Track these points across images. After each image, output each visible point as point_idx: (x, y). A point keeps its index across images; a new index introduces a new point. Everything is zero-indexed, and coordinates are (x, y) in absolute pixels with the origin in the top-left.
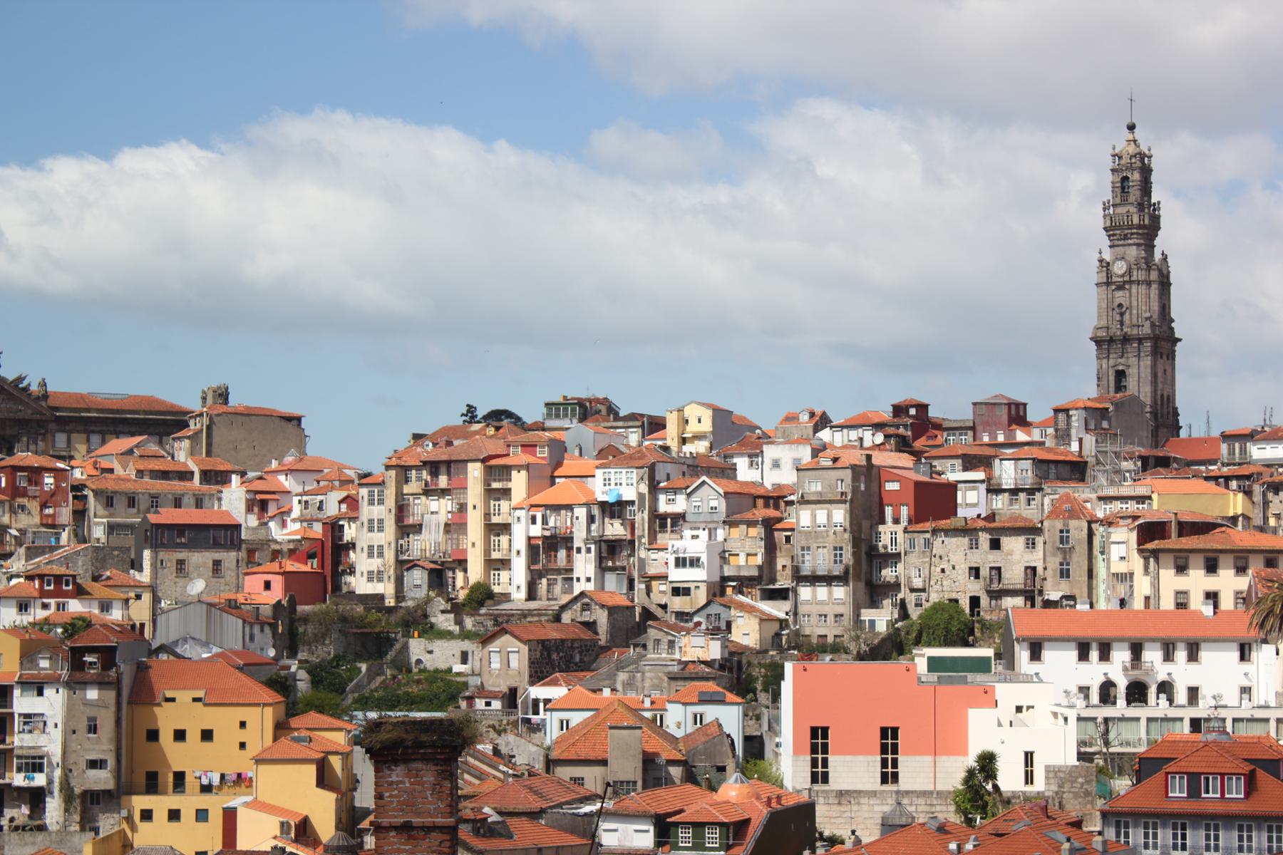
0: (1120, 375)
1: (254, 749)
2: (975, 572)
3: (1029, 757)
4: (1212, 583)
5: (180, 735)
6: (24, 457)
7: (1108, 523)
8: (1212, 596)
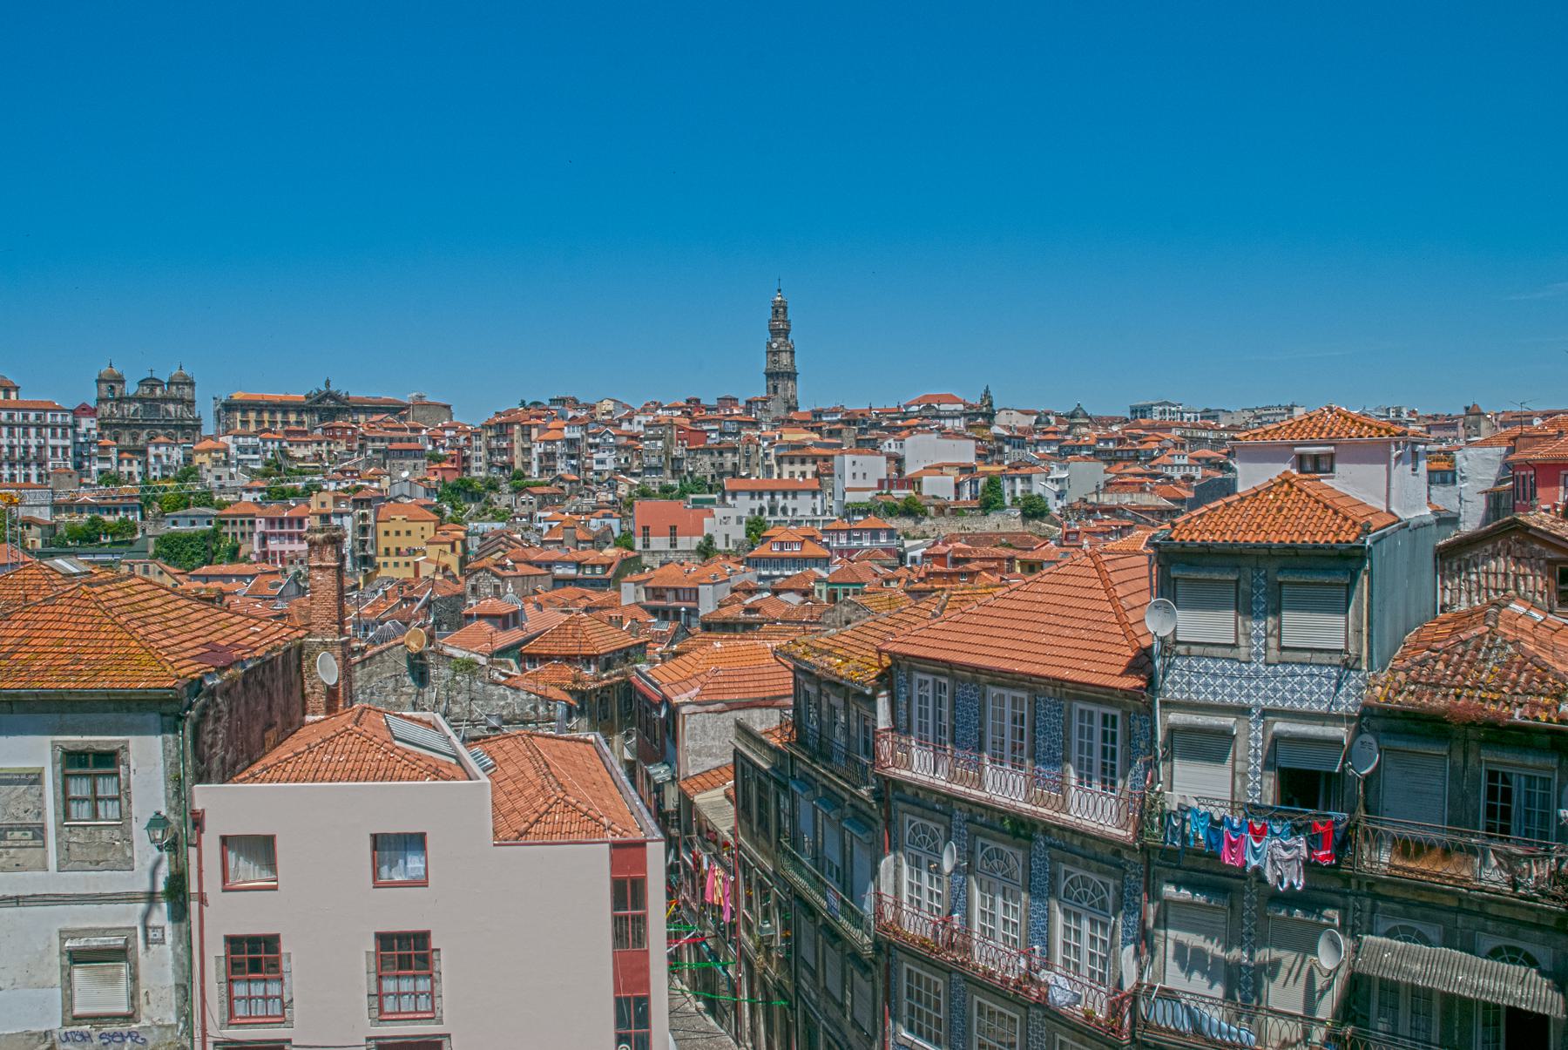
0: (775, 388)
1: (427, 538)
3: (727, 536)
5: (398, 533)
6: (340, 423)
8: (803, 474)
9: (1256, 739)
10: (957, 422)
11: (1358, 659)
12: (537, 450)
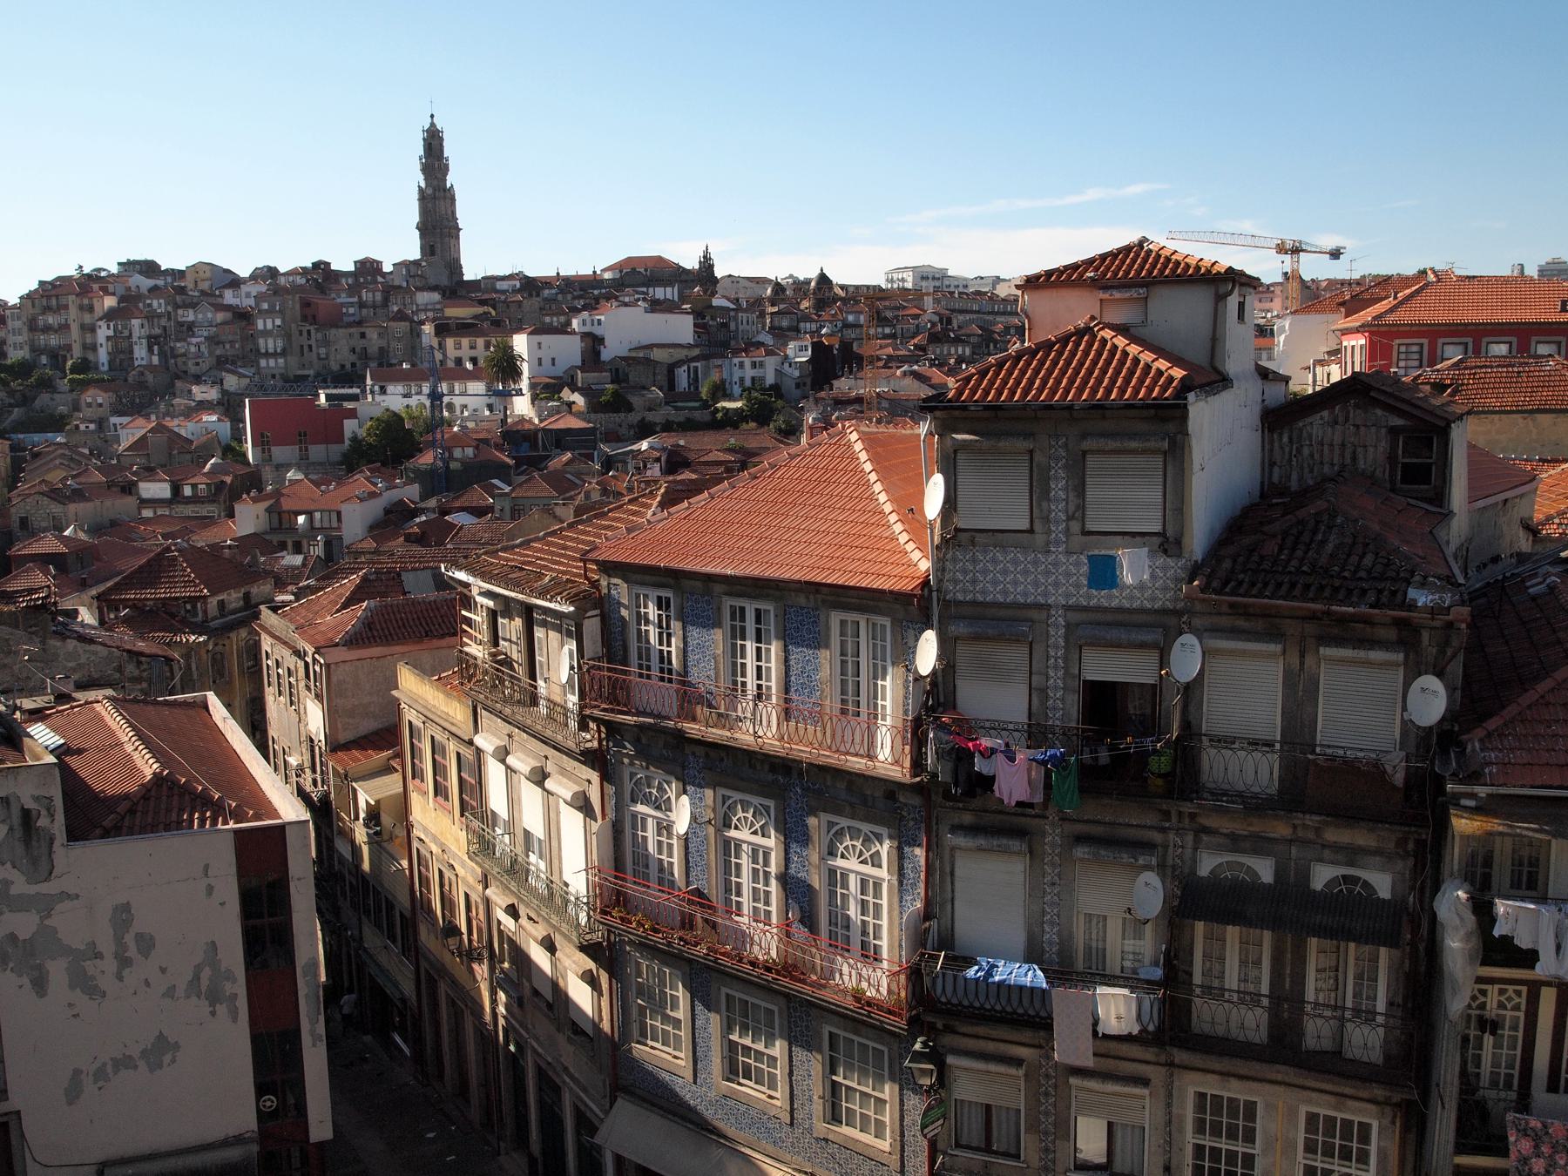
2: (353, 350)
4: (473, 353)
7: (422, 323)
9: (1057, 647)
10: (669, 290)
11: (1178, 542)
12: (103, 332)
